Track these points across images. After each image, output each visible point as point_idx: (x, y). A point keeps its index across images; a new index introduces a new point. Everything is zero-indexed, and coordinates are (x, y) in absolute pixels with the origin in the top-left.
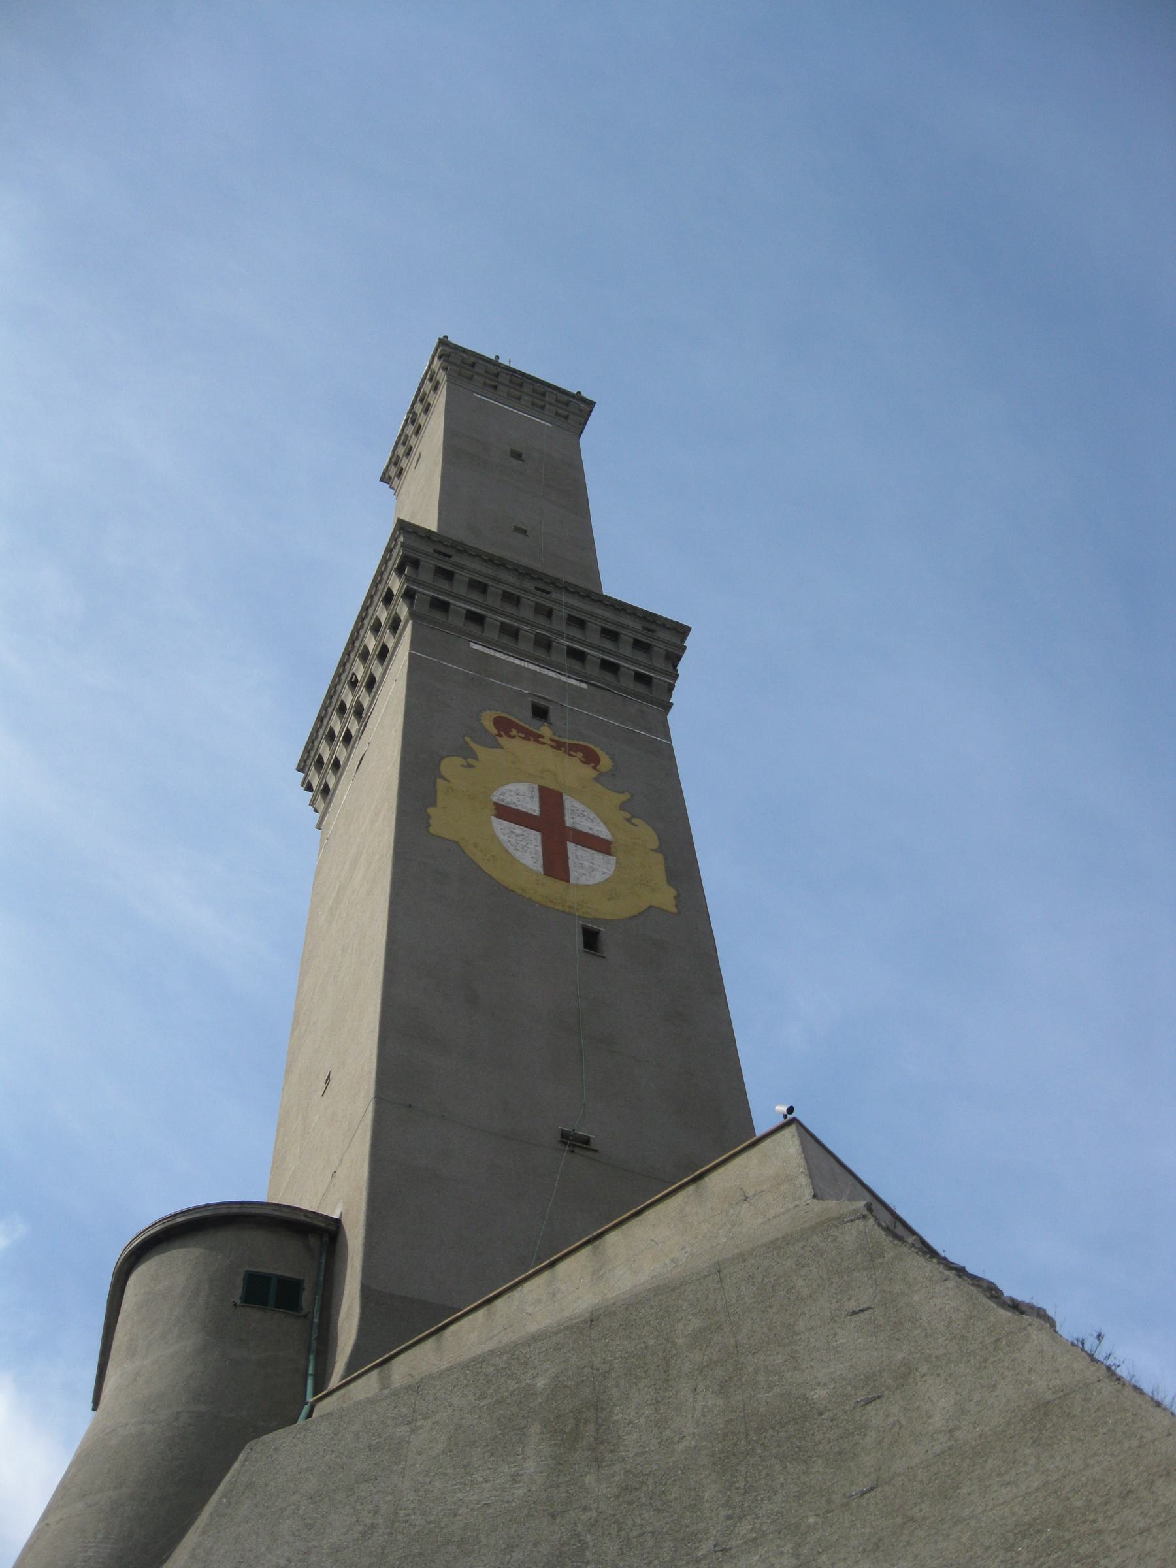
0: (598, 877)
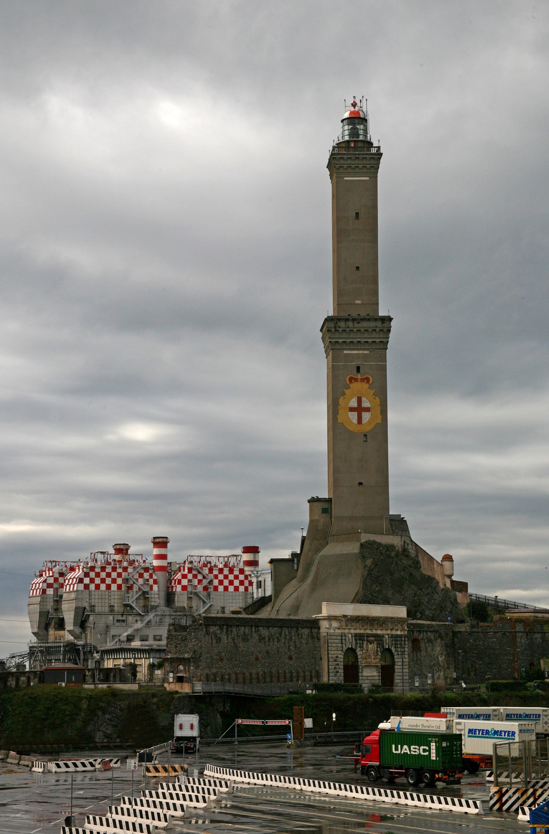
0: (368, 419)
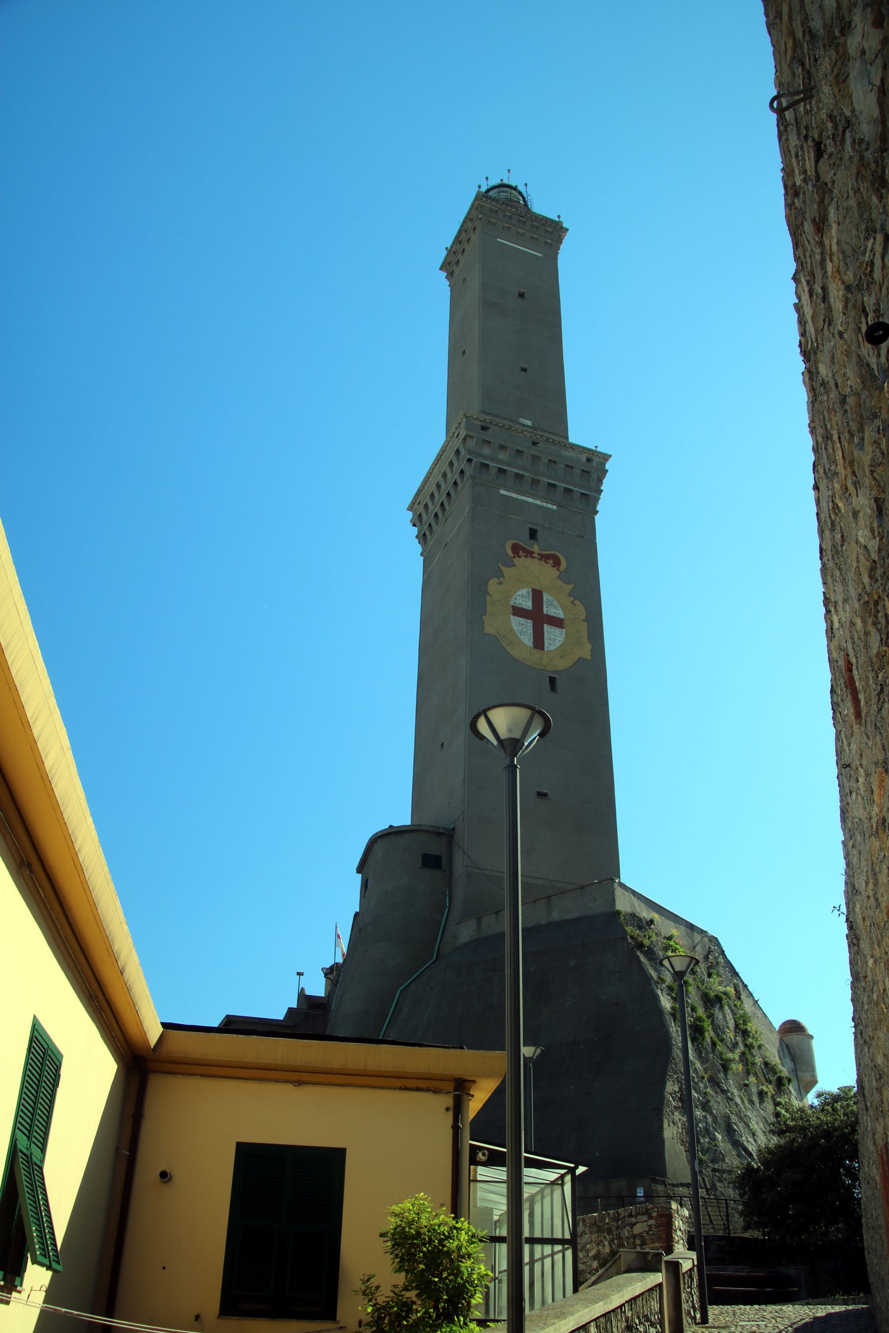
0: (558, 644)
